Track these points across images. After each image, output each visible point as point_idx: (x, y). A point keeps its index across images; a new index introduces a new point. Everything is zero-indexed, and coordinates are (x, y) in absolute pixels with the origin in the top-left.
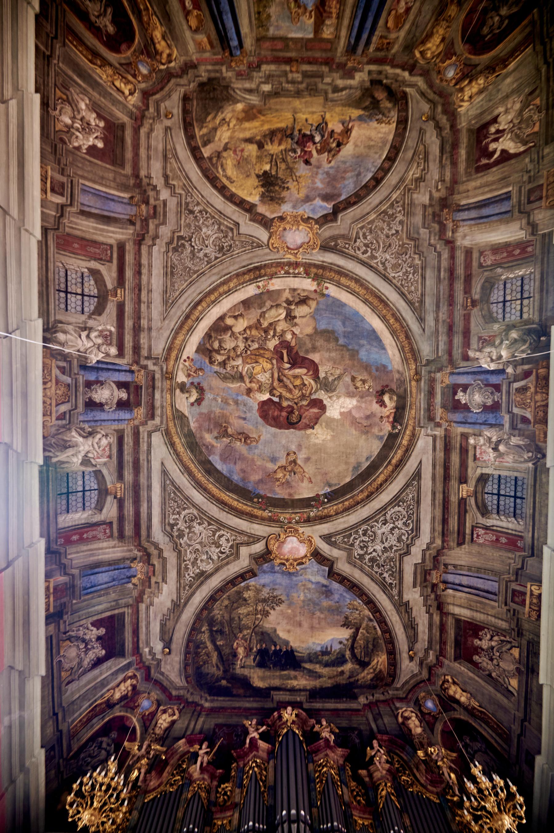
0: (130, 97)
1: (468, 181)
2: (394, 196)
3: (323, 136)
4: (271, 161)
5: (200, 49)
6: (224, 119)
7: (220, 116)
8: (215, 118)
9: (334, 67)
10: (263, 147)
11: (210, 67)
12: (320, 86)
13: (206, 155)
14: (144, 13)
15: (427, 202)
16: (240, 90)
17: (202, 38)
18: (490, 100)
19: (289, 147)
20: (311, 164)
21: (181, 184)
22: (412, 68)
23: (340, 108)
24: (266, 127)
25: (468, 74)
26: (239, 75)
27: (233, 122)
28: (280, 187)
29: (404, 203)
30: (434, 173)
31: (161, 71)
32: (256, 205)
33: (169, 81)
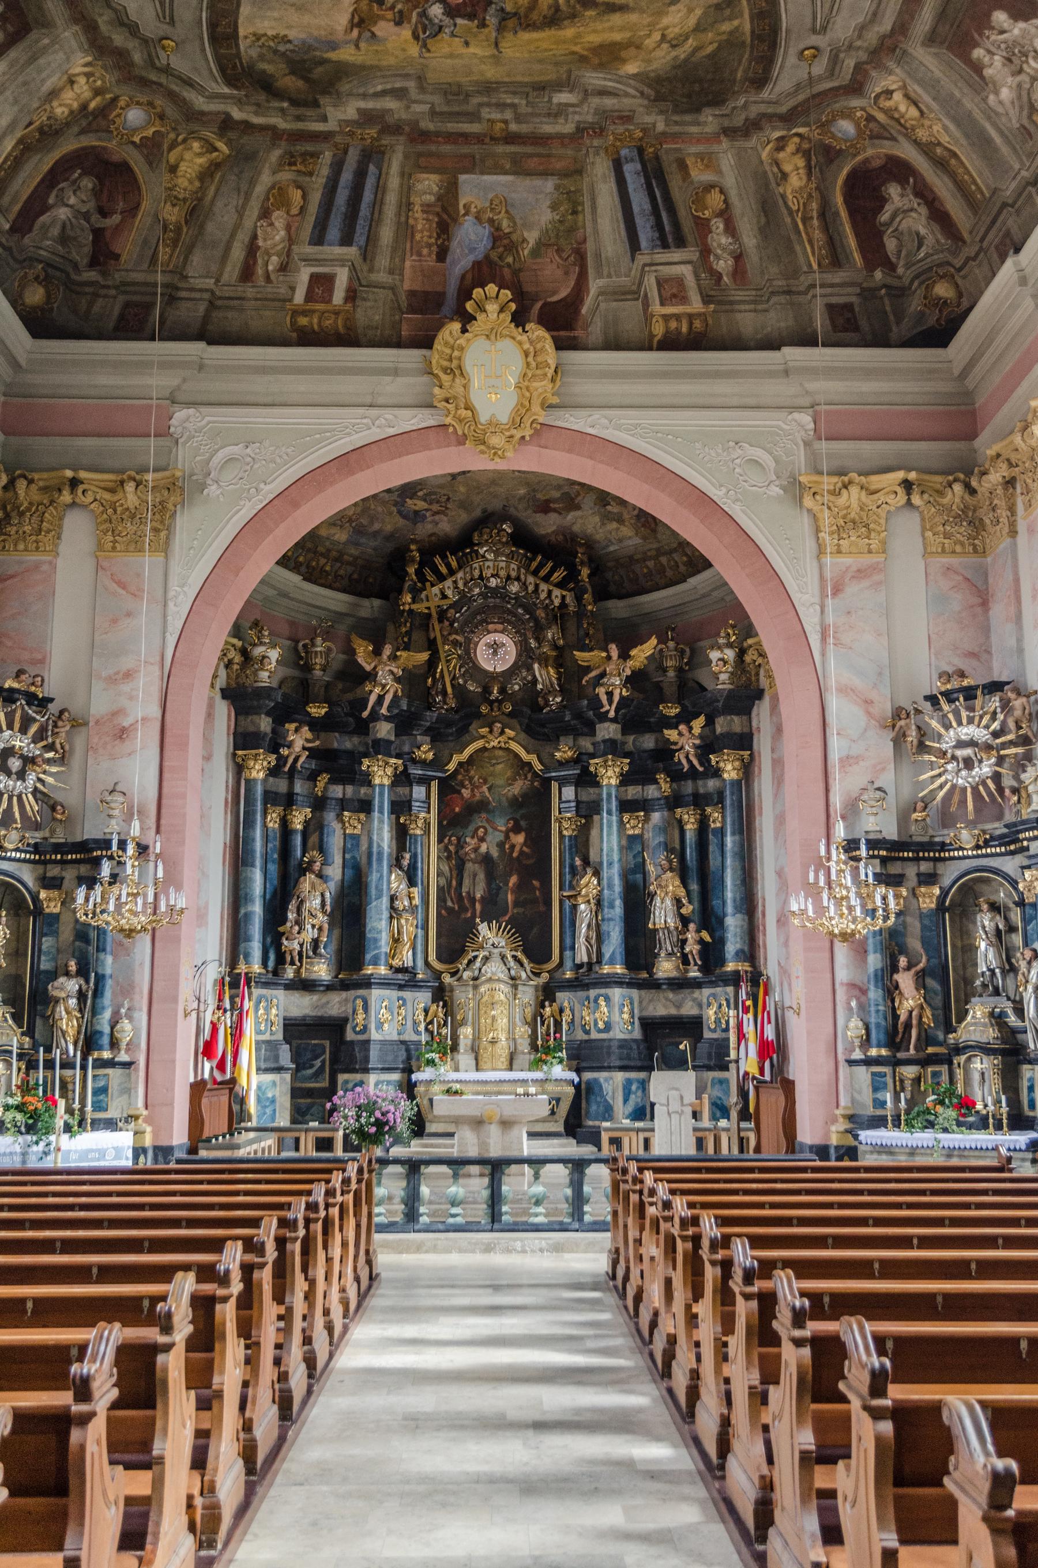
5: (709, 161)
6: (674, 46)
7: (682, 53)
8: (696, 50)
11: (694, 129)
12: (437, 99)
16: (627, 95)
17: (699, 175)
18: (25, 83)
22: (226, 124)
25: (95, 118)
26: (627, 118)
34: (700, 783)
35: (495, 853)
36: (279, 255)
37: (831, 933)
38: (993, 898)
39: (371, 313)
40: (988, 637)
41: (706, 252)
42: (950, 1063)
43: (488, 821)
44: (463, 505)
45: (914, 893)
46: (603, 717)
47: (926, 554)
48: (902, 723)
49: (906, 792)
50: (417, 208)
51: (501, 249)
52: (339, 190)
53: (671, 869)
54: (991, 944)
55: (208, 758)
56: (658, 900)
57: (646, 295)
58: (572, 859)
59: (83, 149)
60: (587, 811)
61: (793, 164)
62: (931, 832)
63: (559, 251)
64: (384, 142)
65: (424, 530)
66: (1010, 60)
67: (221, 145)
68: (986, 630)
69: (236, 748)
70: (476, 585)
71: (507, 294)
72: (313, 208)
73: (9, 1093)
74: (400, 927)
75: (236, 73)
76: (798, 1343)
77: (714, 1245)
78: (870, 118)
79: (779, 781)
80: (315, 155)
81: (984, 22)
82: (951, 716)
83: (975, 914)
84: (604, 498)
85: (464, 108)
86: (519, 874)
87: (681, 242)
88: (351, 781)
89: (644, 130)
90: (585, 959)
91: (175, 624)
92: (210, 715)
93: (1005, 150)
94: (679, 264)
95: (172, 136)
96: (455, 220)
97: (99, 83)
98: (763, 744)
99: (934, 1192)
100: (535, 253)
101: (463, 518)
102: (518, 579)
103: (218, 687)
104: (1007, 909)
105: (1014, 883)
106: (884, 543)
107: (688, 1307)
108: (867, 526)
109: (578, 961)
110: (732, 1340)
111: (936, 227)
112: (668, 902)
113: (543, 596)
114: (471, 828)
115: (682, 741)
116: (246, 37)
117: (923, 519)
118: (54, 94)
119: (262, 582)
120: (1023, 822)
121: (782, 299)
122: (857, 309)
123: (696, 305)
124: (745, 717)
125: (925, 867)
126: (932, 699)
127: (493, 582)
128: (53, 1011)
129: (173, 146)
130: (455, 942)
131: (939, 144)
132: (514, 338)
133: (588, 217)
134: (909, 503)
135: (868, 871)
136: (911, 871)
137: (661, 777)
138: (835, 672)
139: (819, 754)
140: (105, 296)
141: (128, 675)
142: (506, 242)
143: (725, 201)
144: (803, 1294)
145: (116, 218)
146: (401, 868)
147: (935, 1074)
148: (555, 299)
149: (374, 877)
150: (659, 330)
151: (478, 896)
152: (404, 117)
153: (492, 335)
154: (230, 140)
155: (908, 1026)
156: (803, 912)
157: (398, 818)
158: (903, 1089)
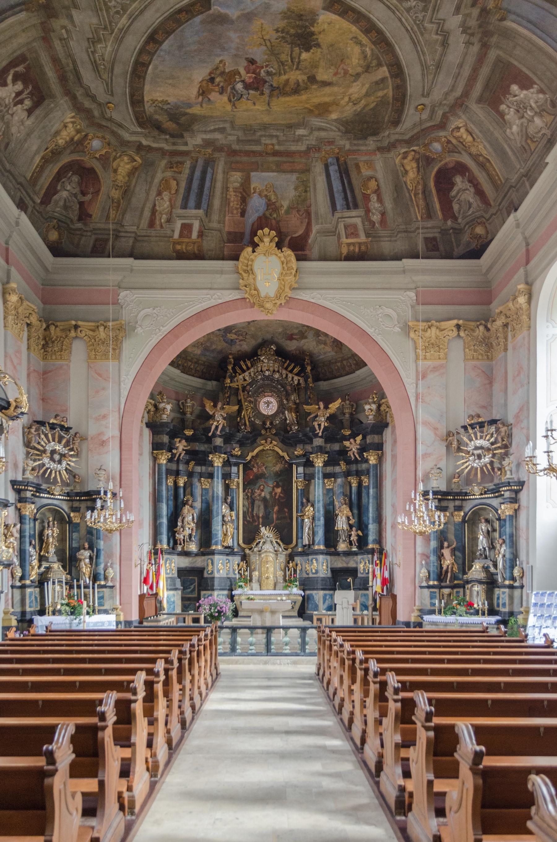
0: (460, 126)
1: (28, 43)
2: (124, 21)
3: (233, 88)
4: (299, 62)
6: (355, 104)
7: (358, 108)
8: (365, 106)
9: (226, 149)
10: (308, 78)
12: (240, 133)
13: (385, 68)
14: (420, 192)
15: (74, 12)
16: (332, 130)
19: (275, 78)
20: (247, 59)
21: (427, 36)
22: (140, 148)
23: (214, 114)
24: (304, 97)
25: (78, 145)
26: (331, 142)
27: (343, 102)
28: (287, 33)
29: (107, 11)
30: (78, 49)
31: (418, 145)
32: (324, 9)
33: (412, 137)
34: (359, 465)
35: (268, 497)
36: (166, 214)
37: (415, 532)
38: (487, 517)
39: (210, 243)
40: (491, 399)
41: (368, 211)
42: (464, 587)
43: (265, 482)
44: (254, 337)
45: (452, 515)
46: (316, 436)
47: (465, 359)
48: (451, 438)
49: (451, 470)
50: (231, 190)
51: (270, 211)
52: (194, 181)
53: (345, 504)
54: (485, 537)
55: (141, 454)
56: (339, 518)
57: (339, 234)
58: (302, 499)
59: (73, 161)
60: (309, 478)
61: (411, 166)
62: (461, 488)
63: (298, 211)
64: (215, 156)
65: (235, 349)
66: (518, 111)
67: (137, 158)
68: (491, 396)
69: (153, 449)
70: (259, 375)
71: (273, 233)
72: (182, 191)
73: (63, 599)
74: (227, 529)
75: (143, 120)
76: (396, 701)
77: (361, 662)
78: (449, 142)
79: (394, 465)
80: (182, 163)
81: (506, 91)
82: (472, 435)
83: (478, 524)
84: (318, 333)
85: (254, 138)
86: (278, 505)
87: (356, 206)
88: (204, 464)
89: (340, 149)
90: (307, 543)
91: (125, 393)
92: (141, 435)
93: (513, 158)
94: (355, 218)
95: (114, 154)
96: (249, 196)
97: (78, 127)
98: (388, 448)
99: (454, 641)
100: (287, 212)
101: (253, 343)
102: (278, 371)
103: (144, 422)
104: (493, 521)
105: (496, 510)
106: (446, 354)
107: (350, 687)
108: (439, 346)
109: (304, 544)
110: (368, 700)
111: (478, 198)
112: (344, 518)
113: (290, 379)
114: (258, 485)
115: (351, 447)
116: (148, 102)
117: (465, 343)
118: (57, 133)
119: (163, 373)
120: (502, 483)
121: (403, 235)
122: (438, 240)
123: (363, 238)
124: (380, 436)
125: (457, 503)
126: (465, 428)
127: (267, 373)
128: (79, 565)
129: (115, 159)
130: (251, 536)
131: (481, 155)
132: (277, 255)
133: (312, 193)
134: (459, 335)
135: (432, 505)
136: (451, 505)
137: (342, 463)
138: (421, 415)
139: (413, 453)
140: (86, 236)
141: (104, 417)
142: (273, 206)
143: (378, 185)
144: (398, 682)
145: (89, 197)
146: (227, 503)
147: (457, 592)
148: (296, 235)
149: (215, 507)
150: (345, 251)
151: (261, 515)
152: (224, 142)
153: (266, 253)
154: (142, 156)
155: (447, 572)
156: (403, 523)
157: (225, 481)
158: (443, 598)
